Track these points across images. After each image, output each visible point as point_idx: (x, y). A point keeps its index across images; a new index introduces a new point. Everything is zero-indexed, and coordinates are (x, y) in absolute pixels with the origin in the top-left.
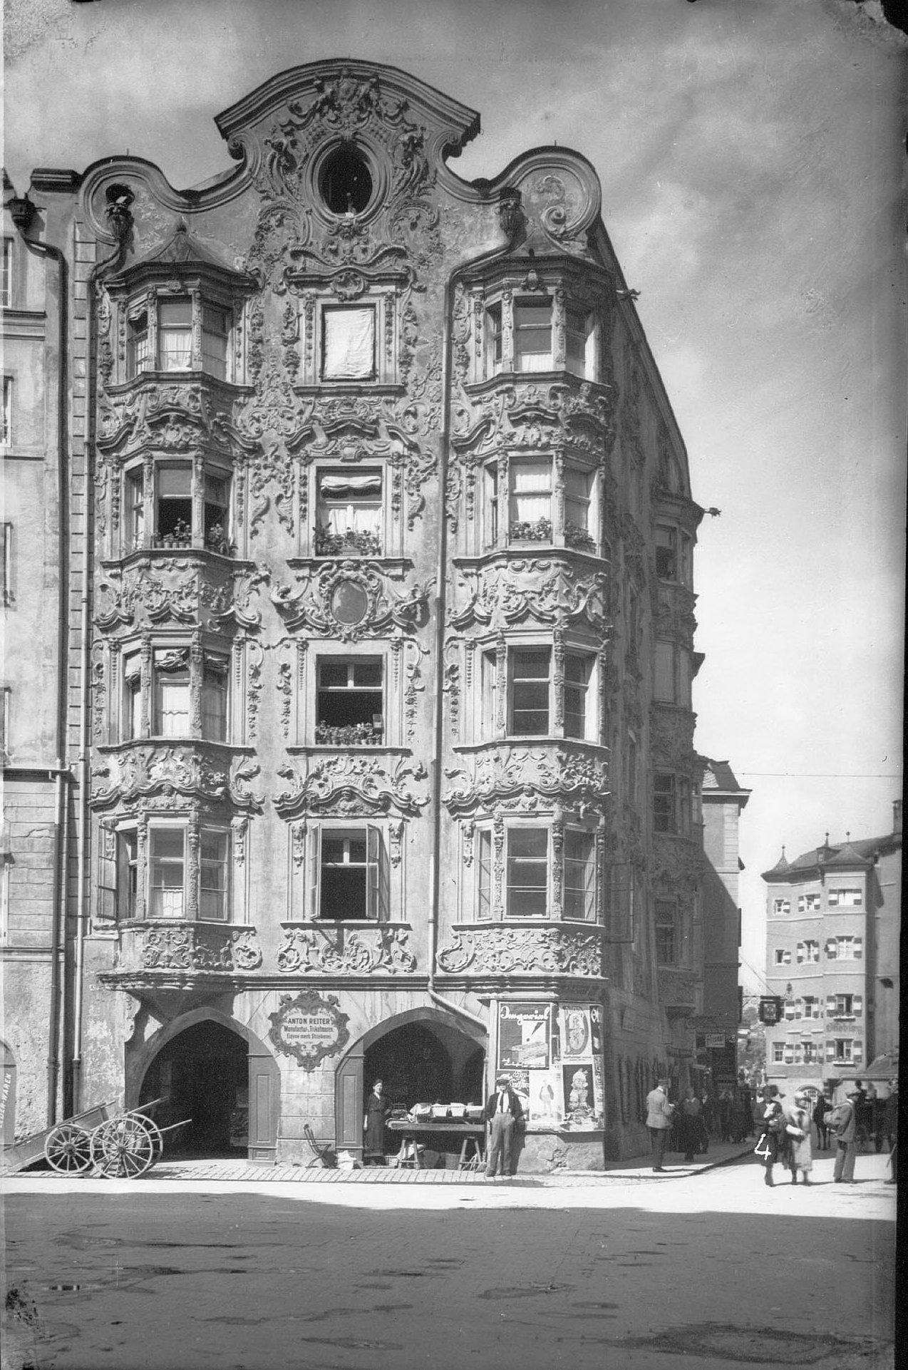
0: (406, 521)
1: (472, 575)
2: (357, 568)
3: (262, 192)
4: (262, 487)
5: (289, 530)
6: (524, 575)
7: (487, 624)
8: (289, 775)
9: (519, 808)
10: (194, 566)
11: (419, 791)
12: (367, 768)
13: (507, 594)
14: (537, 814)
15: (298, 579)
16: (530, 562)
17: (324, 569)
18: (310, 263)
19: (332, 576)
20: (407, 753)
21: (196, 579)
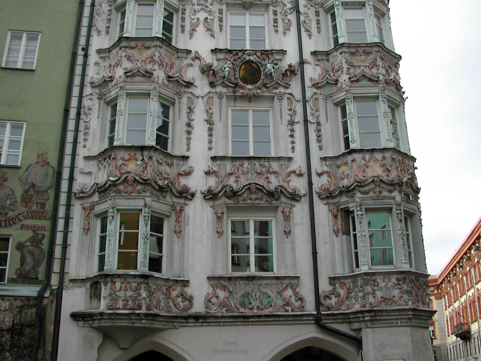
4: (195, 14)
5: (212, 36)
7: (336, 84)
9: (371, 194)
11: (299, 185)
12: (264, 170)
17: (234, 55)
20: (290, 159)
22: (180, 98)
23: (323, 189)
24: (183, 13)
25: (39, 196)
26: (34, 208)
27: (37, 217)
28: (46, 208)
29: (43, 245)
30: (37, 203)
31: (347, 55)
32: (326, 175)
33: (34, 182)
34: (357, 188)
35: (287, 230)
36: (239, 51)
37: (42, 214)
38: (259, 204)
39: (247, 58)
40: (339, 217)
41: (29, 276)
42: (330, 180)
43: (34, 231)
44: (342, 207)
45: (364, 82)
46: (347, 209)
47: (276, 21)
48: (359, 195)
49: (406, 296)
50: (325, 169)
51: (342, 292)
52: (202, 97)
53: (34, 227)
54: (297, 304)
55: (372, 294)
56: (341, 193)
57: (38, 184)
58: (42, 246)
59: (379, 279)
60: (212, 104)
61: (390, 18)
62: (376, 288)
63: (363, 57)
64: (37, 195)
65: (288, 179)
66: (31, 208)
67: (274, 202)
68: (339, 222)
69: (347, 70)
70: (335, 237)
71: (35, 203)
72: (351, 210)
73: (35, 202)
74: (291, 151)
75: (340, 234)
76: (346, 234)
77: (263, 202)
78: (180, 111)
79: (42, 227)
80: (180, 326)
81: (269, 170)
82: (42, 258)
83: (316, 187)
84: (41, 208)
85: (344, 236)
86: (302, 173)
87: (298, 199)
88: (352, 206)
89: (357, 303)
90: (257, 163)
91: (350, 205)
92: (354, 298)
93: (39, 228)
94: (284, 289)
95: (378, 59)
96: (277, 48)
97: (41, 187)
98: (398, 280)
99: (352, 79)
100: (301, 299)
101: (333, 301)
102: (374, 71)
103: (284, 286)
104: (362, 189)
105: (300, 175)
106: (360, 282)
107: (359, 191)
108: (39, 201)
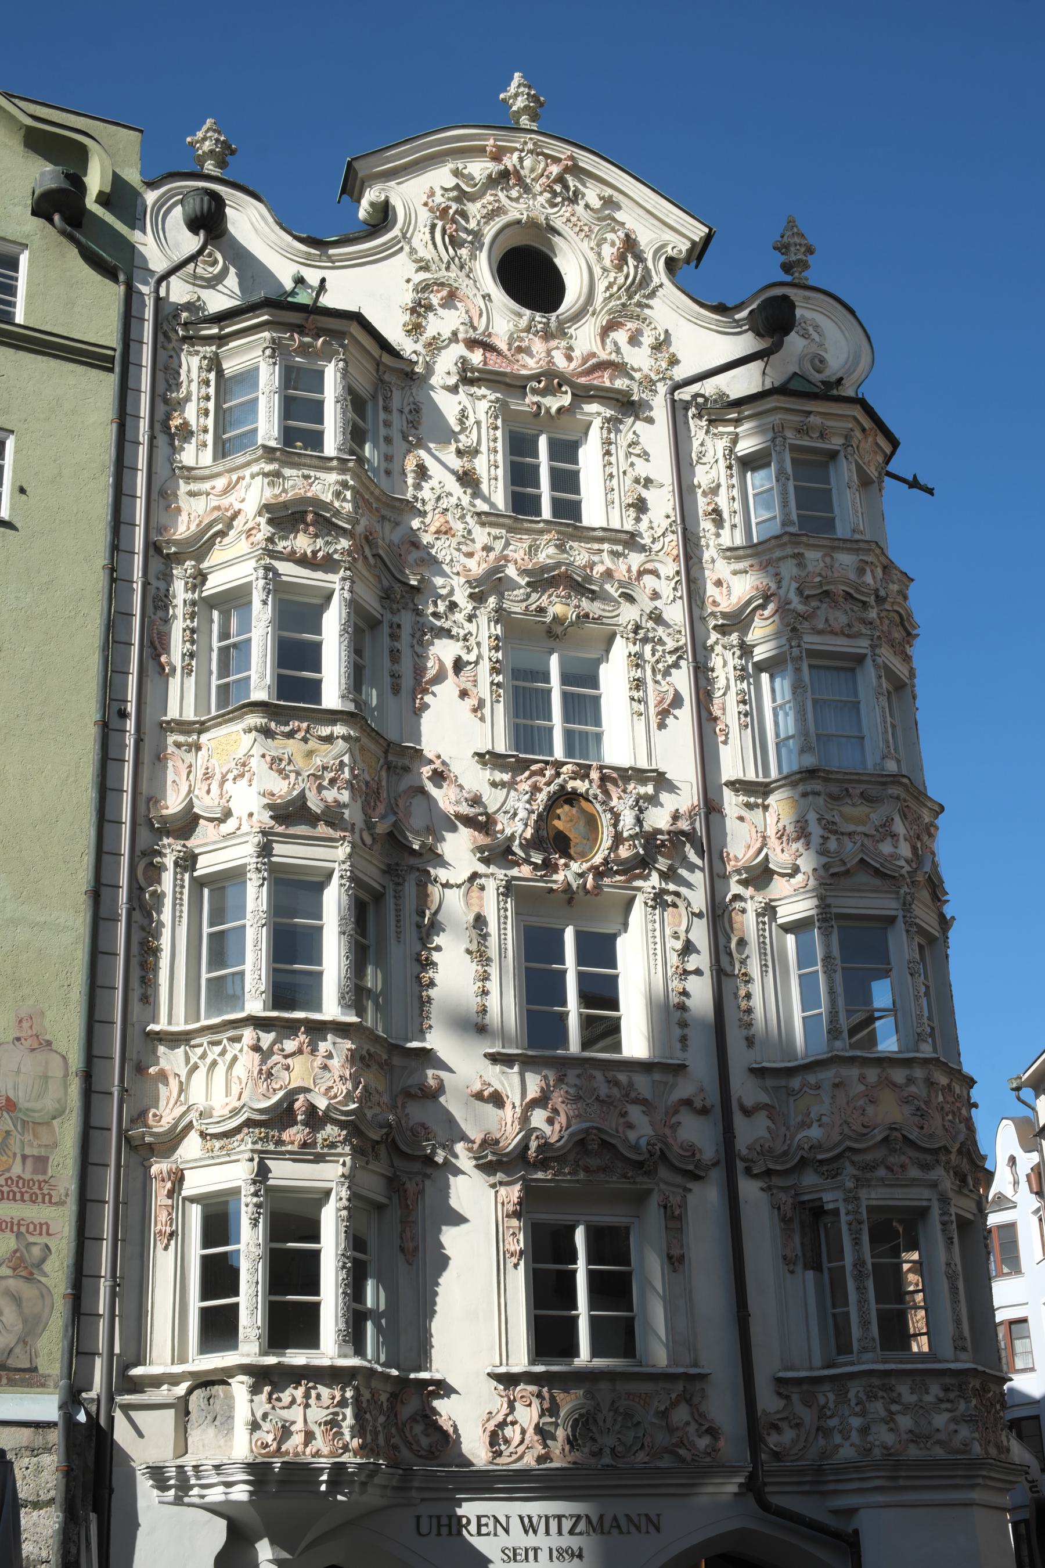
0: (654, 721)
1: (757, 806)
2: (585, 776)
3: (415, 261)
6: (848, 810)
8: (497, 1100)
9: (882, 1172)
10: (344, 738)
12: (616, 1092)
13: (821, 832)
14: (914, 1183)
15: (494, 784)
16: (858, 792)
17: (533, 774)
18: (492, 357)
19: (548, 784)
20: (680, 1069)
21: (346, 759)
22: (398, 884)
23: (759, 1149)
24: (394, 637)
25: (28, 1137)
26: (17, 1169)
27: (26, 1197)
28: (50, 1174)
29: (46, 1275)
30: (24, 1157)
31: (821, 801)
32: (764, 1113)
33: (11, 1095)
34: (847, 1154)
35: (676, 1252)
36: (547, 763)
37: (41, 1189)
38: (607, 1182)
39: (571, 785)
40: (796, 1225)
41: (11, 1362)
42: (773, 1126)
43: (19, 1235)
44: (806, 1198)
45: (863, 878)
46: (817, 1204)
47: (638, 684)
48: (850, 1170)
49: (964, 1432)
50: (764, 1099)
51: (807, 1416)
52: (459, 886)
53: (19, 1225)
54: (703, 1443)
55: (887, 1423)
56: (803, 1163)
57: (23, 1102)
58: (43, 1279)
59: (904, 1389)
60: (482, 906)
61: (914, 698)
62: (895, 1408)
63: (861, 810)
64: (23, 1134)
65: (674, 1120)
66: (8, 1170)
67: (639, 1179)
68: (797, 1238)
69: (821, 841)
70: (788, 1274)
71: (19, 1159)
72: (829, 1207)
73: (18, 1151)
74: (678, 1045)
75: (799, 1268)
76: (813, 1268)
77: (615, 1179)
78: (398, 921)
79: (41, 1225)
80: (423, 1500)
81: (627, 1095)
82: (47, 1310)
83: (742, 1144)
84: (35, 1171)
85: (810, 1274)
86: (708, 1104)
87: (702, 1174)
88: (831, 1199)
89: (847, 1444)
90: (598, 1075)
91: (827, 1197)
92: (840, 1432)
93: (31, 1227)
94: (674, 1405)
95: (897, 819)
96: (643, 764)
97: (33, 1111)
98: (946, 1389)
99: (832, 871)
100: (713, 1432)
101: (788, 1435)
102: (886, 848)
103: (674, 1396)
104: (856, 1158)
105: (704, 1111)
106: (855, 1390)
107: (853, 1163)
108: (28, 1151)
